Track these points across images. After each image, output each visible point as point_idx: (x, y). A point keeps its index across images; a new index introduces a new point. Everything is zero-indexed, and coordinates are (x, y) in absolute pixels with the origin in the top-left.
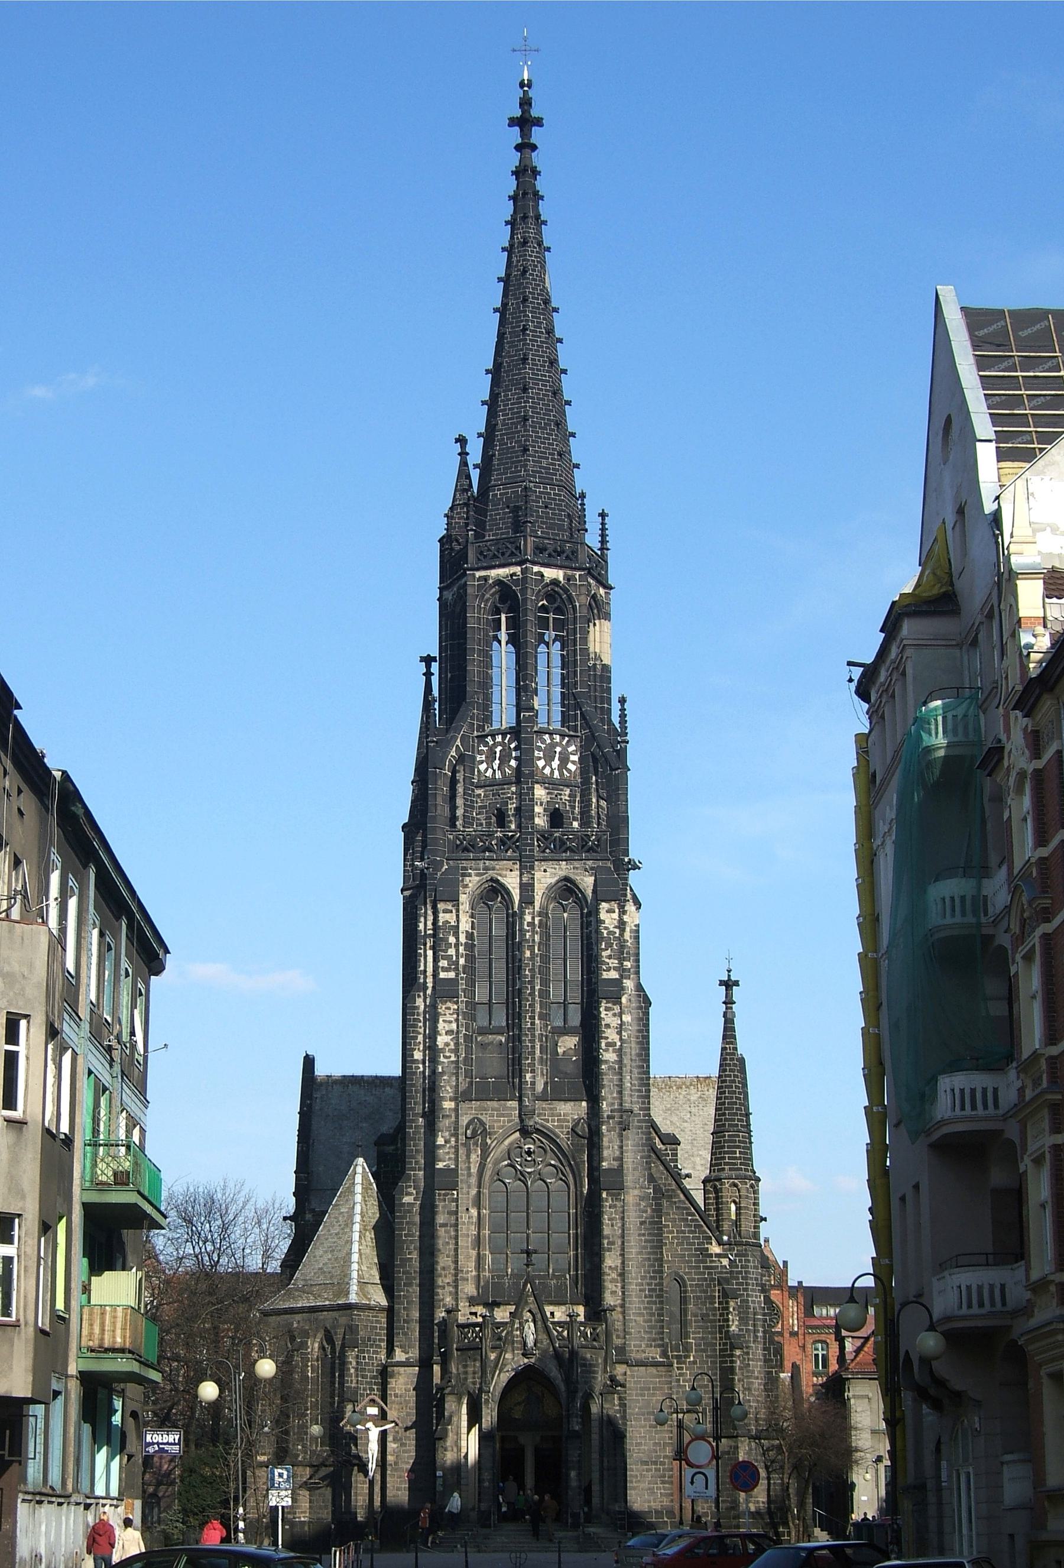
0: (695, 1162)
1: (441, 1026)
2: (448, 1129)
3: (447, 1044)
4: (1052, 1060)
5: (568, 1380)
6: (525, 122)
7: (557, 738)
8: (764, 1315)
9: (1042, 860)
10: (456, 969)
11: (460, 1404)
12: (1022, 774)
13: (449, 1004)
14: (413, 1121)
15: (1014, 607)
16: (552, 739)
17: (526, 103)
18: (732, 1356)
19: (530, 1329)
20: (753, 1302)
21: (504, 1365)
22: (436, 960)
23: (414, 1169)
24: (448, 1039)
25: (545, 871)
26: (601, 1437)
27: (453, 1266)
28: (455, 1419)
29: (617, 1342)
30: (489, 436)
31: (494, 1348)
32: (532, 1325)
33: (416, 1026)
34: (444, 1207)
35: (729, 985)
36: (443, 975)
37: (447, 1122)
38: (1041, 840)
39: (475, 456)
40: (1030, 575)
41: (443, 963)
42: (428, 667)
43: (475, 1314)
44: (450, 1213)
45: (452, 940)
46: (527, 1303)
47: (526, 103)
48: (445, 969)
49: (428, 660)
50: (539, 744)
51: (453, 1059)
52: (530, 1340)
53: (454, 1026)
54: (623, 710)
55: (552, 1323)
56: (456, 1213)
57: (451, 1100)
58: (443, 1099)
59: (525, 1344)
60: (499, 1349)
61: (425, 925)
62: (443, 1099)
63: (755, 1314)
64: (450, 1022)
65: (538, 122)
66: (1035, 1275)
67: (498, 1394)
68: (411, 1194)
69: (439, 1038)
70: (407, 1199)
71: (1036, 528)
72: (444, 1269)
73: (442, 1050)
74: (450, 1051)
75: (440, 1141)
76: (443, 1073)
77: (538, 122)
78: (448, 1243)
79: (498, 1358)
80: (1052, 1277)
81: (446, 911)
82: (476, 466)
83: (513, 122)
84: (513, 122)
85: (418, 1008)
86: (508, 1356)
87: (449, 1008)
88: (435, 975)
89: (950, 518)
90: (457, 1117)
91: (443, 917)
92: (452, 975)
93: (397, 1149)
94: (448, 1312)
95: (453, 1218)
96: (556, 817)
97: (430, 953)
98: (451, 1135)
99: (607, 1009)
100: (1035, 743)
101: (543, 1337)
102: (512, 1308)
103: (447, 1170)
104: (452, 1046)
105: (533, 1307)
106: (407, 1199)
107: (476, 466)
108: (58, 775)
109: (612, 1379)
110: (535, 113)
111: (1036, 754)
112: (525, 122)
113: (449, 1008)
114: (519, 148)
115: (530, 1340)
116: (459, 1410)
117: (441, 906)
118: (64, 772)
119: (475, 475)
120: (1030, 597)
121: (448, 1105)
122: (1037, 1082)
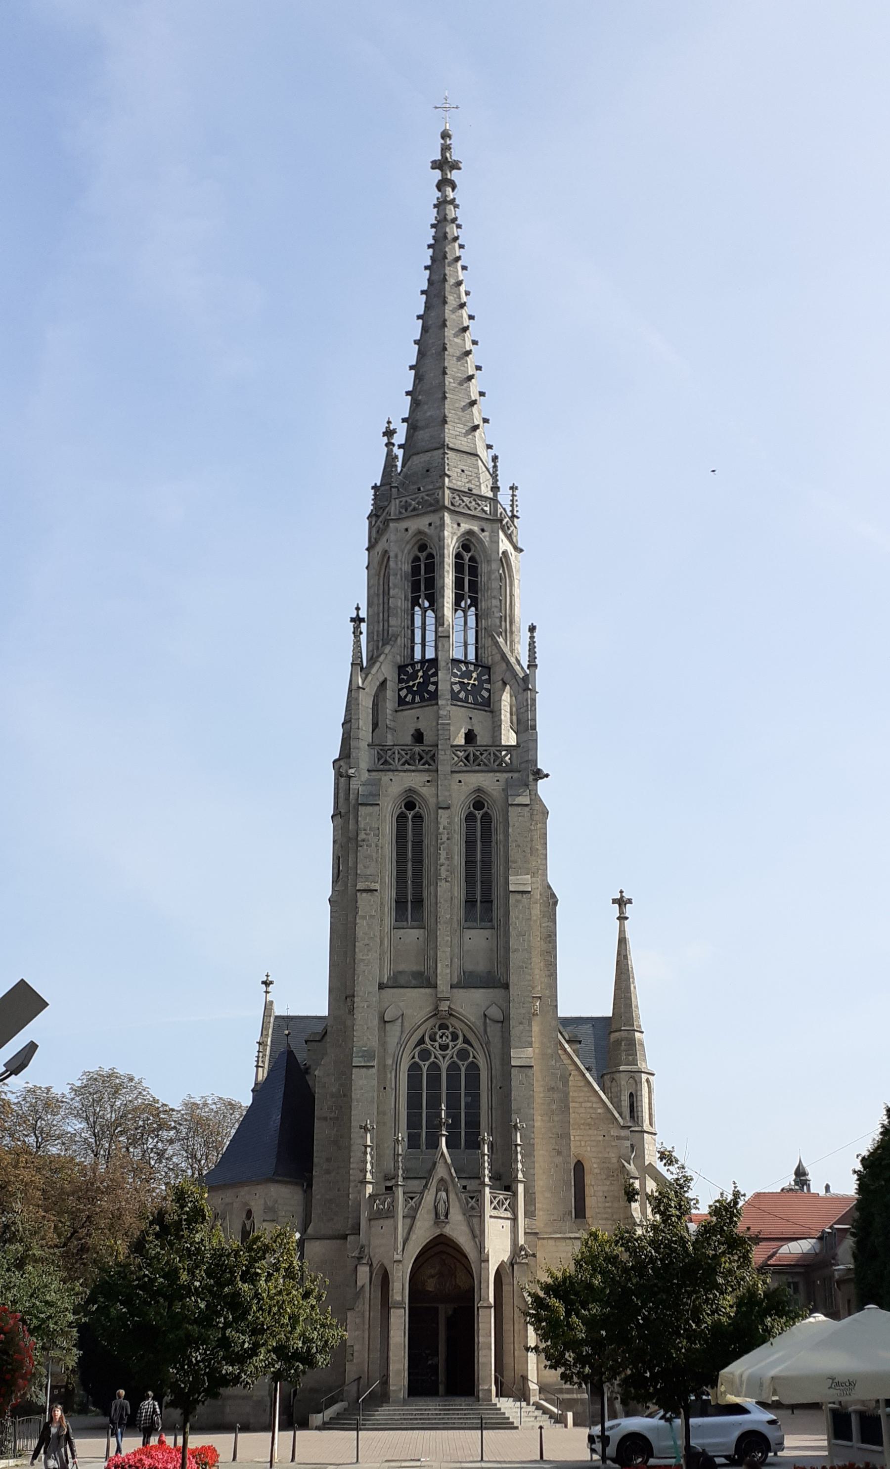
6: (444, 164)
7: (472, 668)
16: (467, 667)
17: (445, 148)
25: (460, 782)
30: (411, 422)
35: (621, 902)
39: (400, 438)
47: (445, 148)
50: (455, 671)
54: (532, 637)
65: (455, 166)
77: (455, 166)
82: (400, 446)
83: (436, 165)
84: (436, 165)
96: (470, 737)
102: (424, 1181)
107: (400, 446)
110: (454, 155)
112: (444, 164)
114: (440, 186)
119: (400, 453)
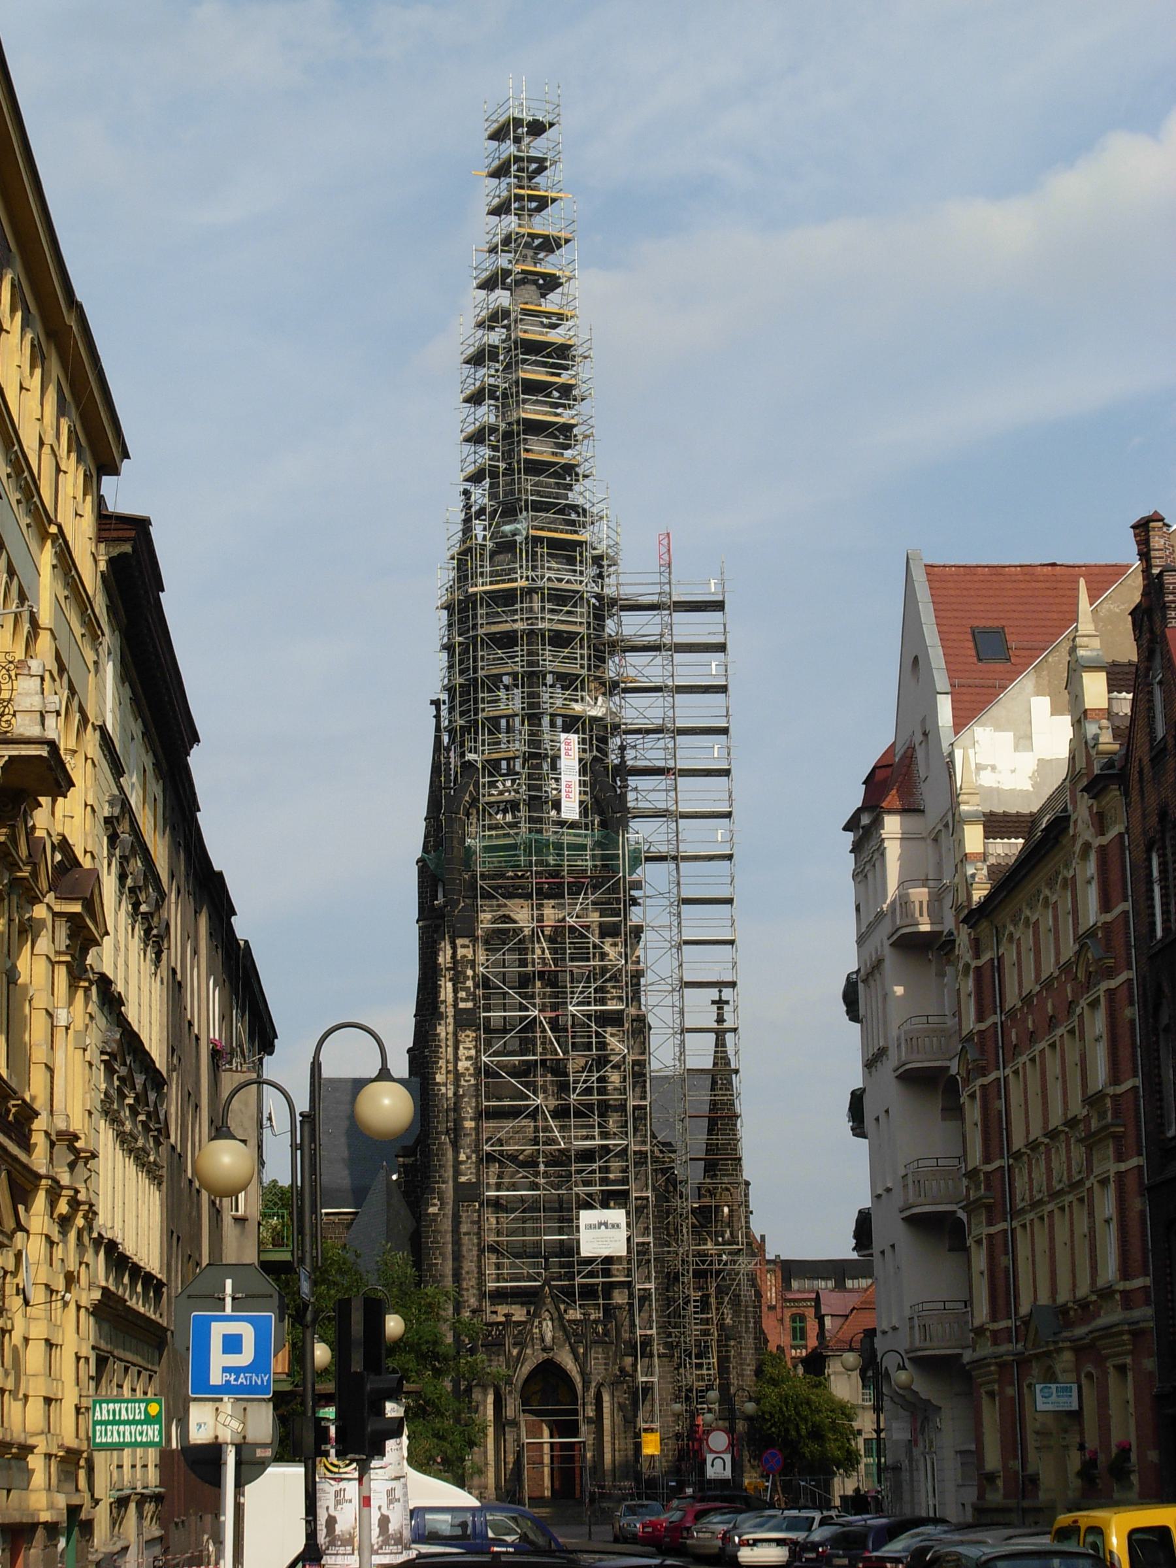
0: (691, 1174)
1: (461, 1051)
2: (469, 1146)
3: (467, 1069)
4: (987, 1174)
5: (583, 1373)
8: (755, 1307)
9: (981, 1032)
10: (474, 1000)
11: (485, 1395)
12: (967, 966)
13: (468, 1032)
14: (436, 1139)
15: (961, 842)
18: (727, 1346)
19: (548, 1326)
20: (745, 1296)
21: (525, 1360)
22: (455, 991)
23: (438, 1182)
24: (468, 1064)
26: (613, 1422)
27: (476, 1270)
28: (481, 1408)
29: (626, 1336)
31: (515, 1344)
32: (550, 1323)
33: (438, 1052)
34: (468, 1217)
36: (462, 1005)
37: (468, 1140)
38: (980, 1018)
40: (972, 819)
41: (462, 994)
42: (438, 710)
43: (495, 1312)
44: (473, 1222)
45: (470, 973)
46: (544, 1304)
48: (463, 1000)
49: (436, 703)
51: (473, 1082)
52: (549, 1336)
53: (473, 1052)
55: (569, 1321)
56: (479, 1222)
57: (471, 1119)
58: (464, 1119)
59: (543, 1340)
60: (520, 1344)
61: (444, 958)
62: (464, 1119)
63: (747, 1307)
64: (470, 1049)
66: (977, 1323)
67: (520, 1384)
68: (435, 1205)
69: (460, 1064)
70: (432, 1210)
71: (979, 768)
72: (468, 1273)
73: (463, 1075)
74: (470, 1075)
75: (462, 1157)
76: (463, 1096)
78: (471, 1250)
79: (520, 1354)
80: (987, 1326)
81: (463, 946)
85: (439, 1035)
86: (529, 1351)
87: (468, 1036)
88: (455, 1005)
89: (919, 737)
90: (477, 1134)
91: (461, 952)
92: (470, 1005)
93: (416, 1160)
94: (473, 1312)
95: (476, 1226)
97: (450, 985)
98: (473, 1152)
99: (612, 1035)
100: (977, 948)
101: (560, 1334)
103: (468, 1184)
104: (472, 1071)
105: (551, 1307)
106: (432, 1210)
108: (242, 943)
109: (622, 1370)
111: (977, 956)
113: (468, 1036)
115: (549, 1336)
116: (485, 1401)
117: (459, 942)
118: (246, 942)
120: (973, 838)
121: (469, 1124)
122: (978, 1188)
